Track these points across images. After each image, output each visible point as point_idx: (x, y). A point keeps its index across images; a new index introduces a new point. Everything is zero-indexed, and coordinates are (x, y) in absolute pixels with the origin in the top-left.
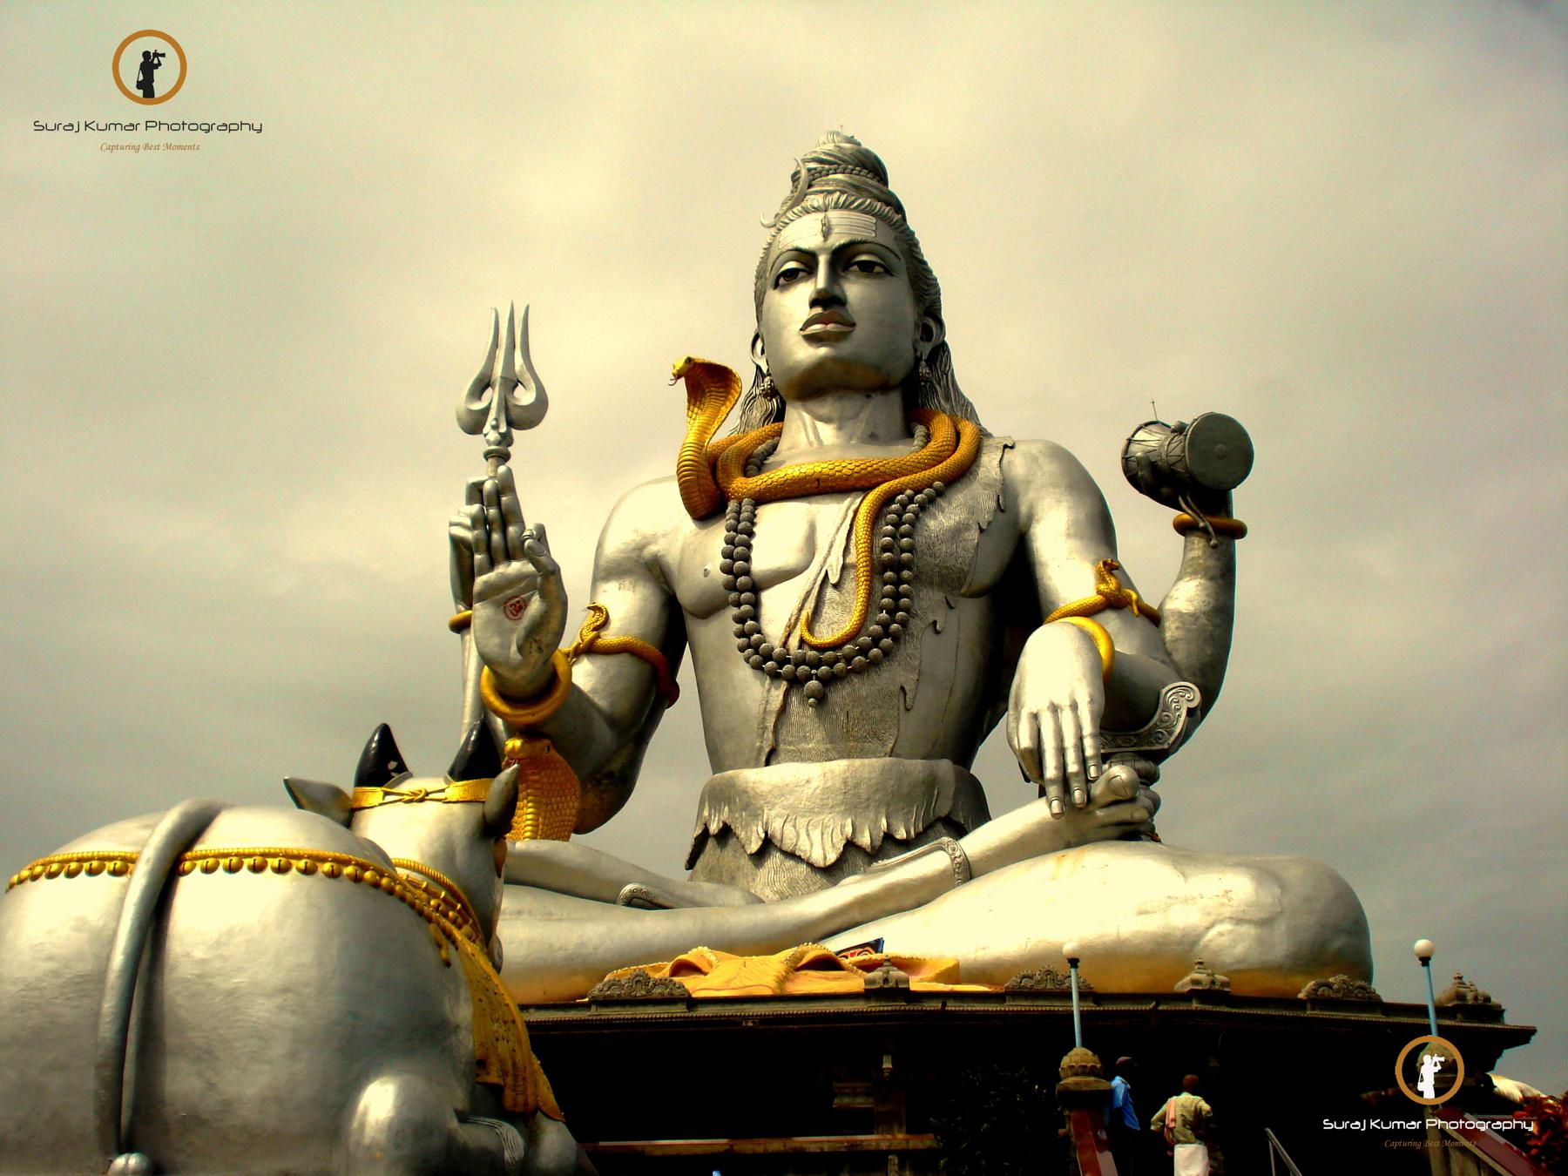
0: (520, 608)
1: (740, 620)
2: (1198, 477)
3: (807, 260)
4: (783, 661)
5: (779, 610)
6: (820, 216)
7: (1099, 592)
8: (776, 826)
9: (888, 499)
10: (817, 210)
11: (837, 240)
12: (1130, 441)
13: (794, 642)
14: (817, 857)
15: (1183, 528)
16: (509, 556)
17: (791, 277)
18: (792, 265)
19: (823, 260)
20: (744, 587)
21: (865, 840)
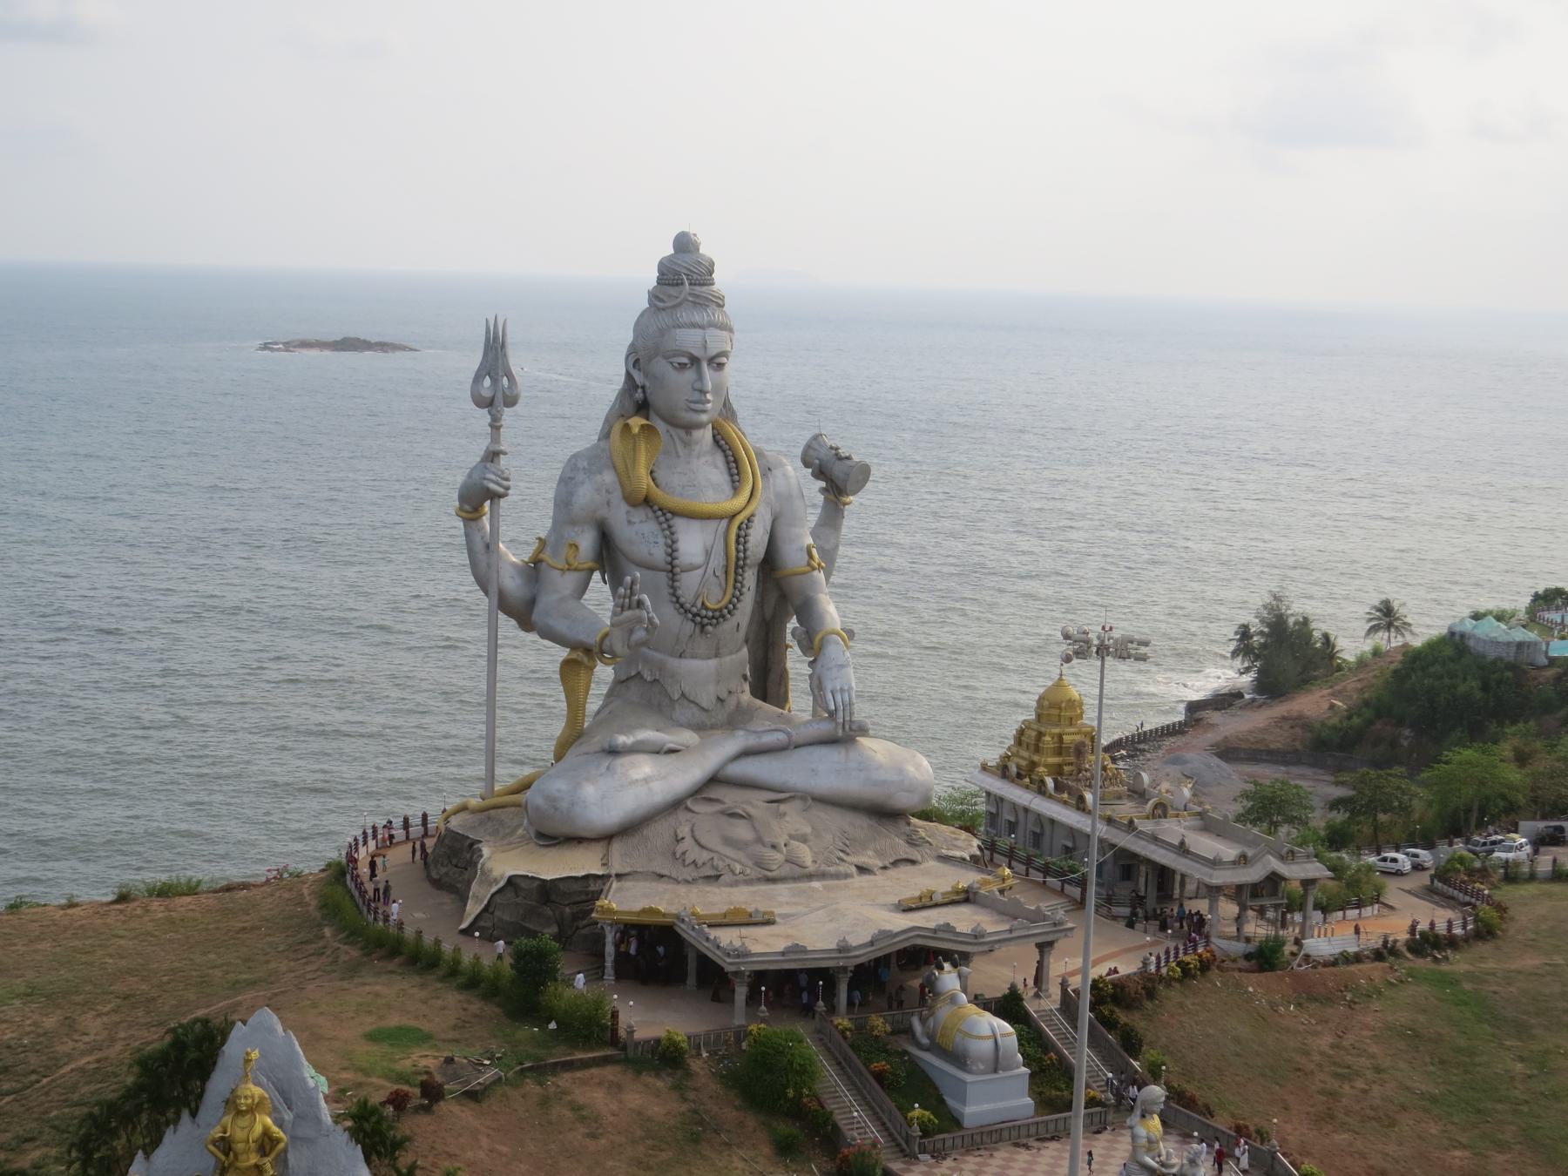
0: (631, 631)
1: (672, 587)
2: (836, 478)
3: (695, 361)
4: (695, 615)
5: (689, 584)
6: (699, 331)
7: (809, 564)
8: (687, 690)
9: (739, 528)
10: (702, 327)
11: (712, 352)
12: (808, 447)
13: (699, 604)
14: (704, 705)
15: (823, 491)
16: (630, 608)
17: (682, 366)
18: (685, 360)
19: (705, 365)
20: (672, 569)
21: (724, 695)
